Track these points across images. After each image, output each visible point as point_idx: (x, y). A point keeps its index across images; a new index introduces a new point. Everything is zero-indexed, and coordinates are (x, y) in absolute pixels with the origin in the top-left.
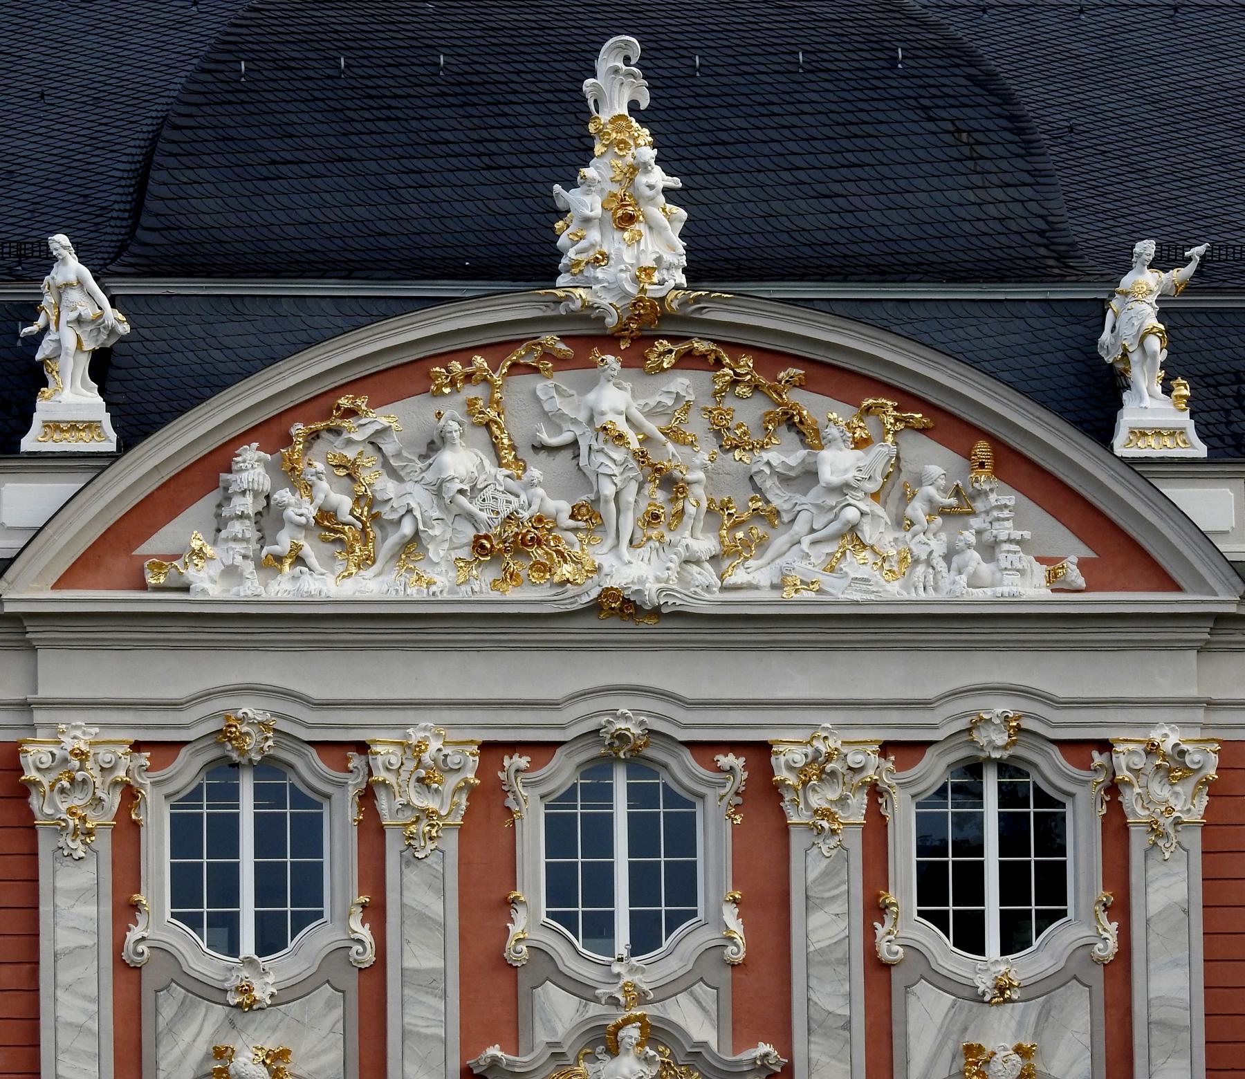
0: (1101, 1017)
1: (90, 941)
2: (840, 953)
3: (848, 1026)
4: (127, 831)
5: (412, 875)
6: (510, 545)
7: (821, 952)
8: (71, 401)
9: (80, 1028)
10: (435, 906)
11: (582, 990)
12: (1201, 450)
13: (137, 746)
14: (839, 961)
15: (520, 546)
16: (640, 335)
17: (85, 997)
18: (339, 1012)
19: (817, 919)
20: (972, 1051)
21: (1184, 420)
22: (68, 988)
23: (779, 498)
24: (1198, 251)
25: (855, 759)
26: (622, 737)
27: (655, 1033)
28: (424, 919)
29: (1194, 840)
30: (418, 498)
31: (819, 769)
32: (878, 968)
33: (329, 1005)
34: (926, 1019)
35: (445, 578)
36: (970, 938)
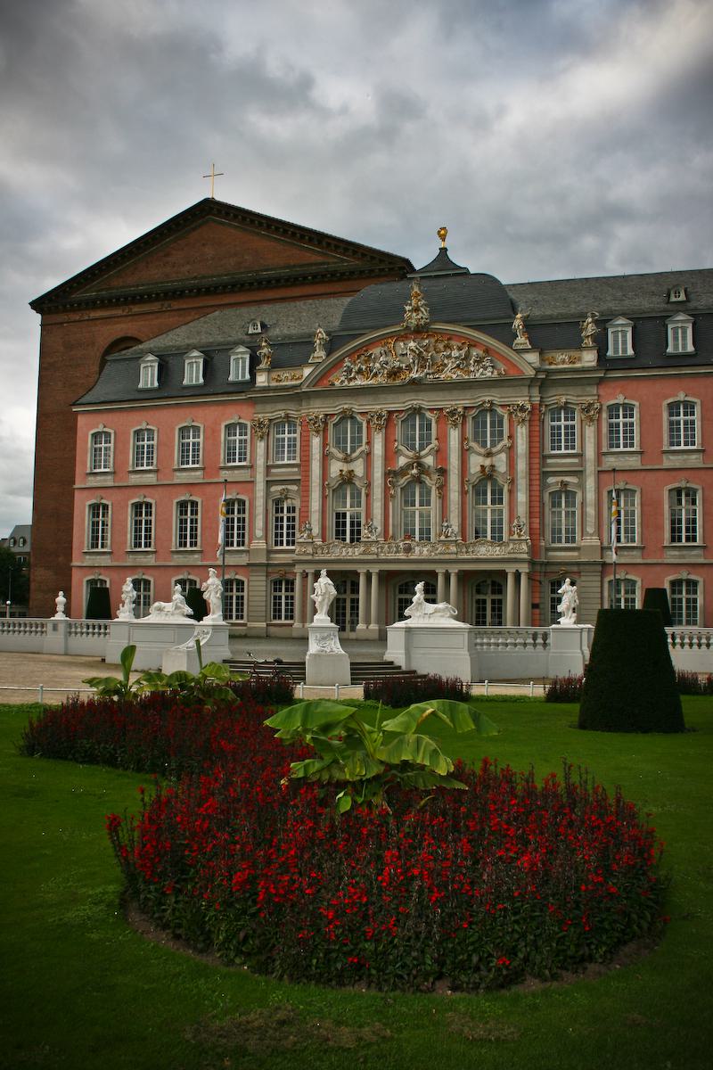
4: (325, 430)
6: (394, 373)
8: (320, 354)
11: (407, 457)
12: (530, 347)
13: (327, 415)
15: (395, 374)
16: (419, 331)
20: (482, 466)
21: (527, 341)
23: (446, 361)
25: (459, 410)
26: (415, 409)
27: (420, 465)
29: (527, 424)
30: (377, 365)
31: (452, 413)
32: (464, 453)
35: (381, 380)
36: (484, 444)
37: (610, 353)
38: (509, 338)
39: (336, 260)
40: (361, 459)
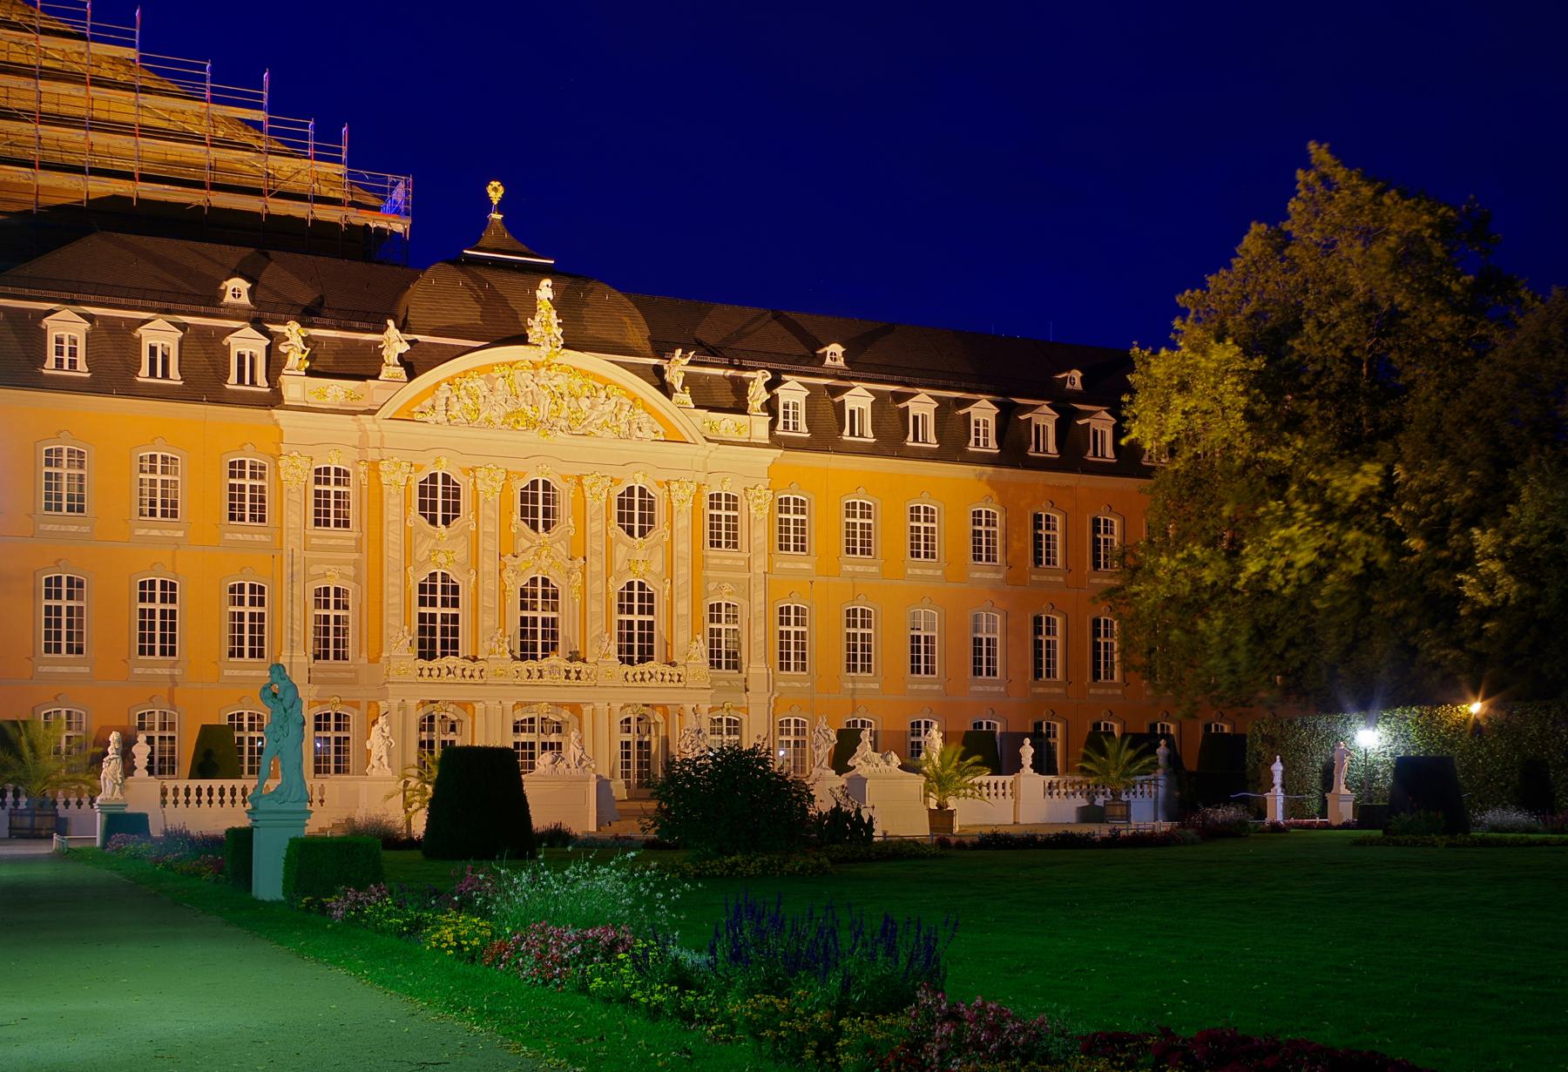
34: (621, 552)
37: (780, 426)
38: (666, 389)
39: (252, 170)
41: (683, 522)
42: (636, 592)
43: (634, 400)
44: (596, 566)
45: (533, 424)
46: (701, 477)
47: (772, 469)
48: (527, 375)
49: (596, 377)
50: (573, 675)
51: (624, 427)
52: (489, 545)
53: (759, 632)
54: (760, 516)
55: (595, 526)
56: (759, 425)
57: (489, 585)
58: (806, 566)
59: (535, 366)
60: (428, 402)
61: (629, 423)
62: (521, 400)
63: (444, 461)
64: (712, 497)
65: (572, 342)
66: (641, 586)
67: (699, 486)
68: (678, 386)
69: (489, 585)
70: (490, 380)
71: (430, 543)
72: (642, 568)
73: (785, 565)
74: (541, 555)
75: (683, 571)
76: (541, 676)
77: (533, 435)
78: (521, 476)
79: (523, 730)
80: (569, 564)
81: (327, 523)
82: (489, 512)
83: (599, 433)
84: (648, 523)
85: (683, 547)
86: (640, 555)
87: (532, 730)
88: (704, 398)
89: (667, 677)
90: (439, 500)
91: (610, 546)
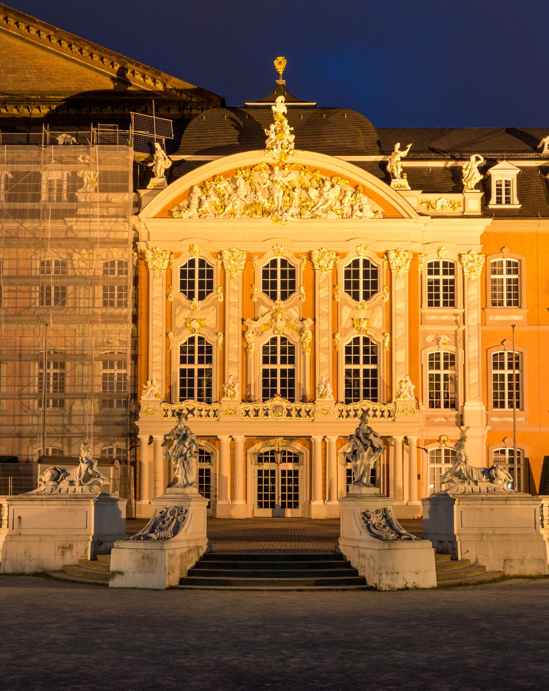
0: (385, 314)
1: (160, 295)
2: (326, 298)
3: (328, 315)
5: (232, 281)
7: (322, 298)
9: (158, 314)
10: (236, 288)
14: (326, 300)
17: (159, 308)
18: (215, 311)
19: (321, 291)
22: (155, 306)
24: (409, 146)
28: (234, 291)
33: (213, 310)
34: (346, 314)
40: (213, 307)
41: (400, 285)
42: (361, 346)
43: (356, 187)
44: (324, 324)
45: (266, 213)
46: (417, 248)
47: (485, 238)
48: (265, 175)
49: (324, 171)
50: (294, 413)
51: (347, 210)
52: (234, 313)
53: (474, 376)
54: (473, 277)
55: (323, 293)
56: (473, 201)
57: (234, 344)
58: (517, 318)
59: (271, 167)
60: (185, 203)
61: (352, 206)
62: (259, 193)
63: (196, 248)
64: (430, 265)
65: (301, 145)
66: (366, 340)
67: (416, 256)
68: (397, 173)
69: (234, 344)
70: (234, 181)
71: (186, 314)
72: (364, 325)
73: (498, 318)
74: (282, 318)
75: (401, 327)
76: (267, 414)
77: (267, 221)
78: (261, 256)
79: (266, 460)
80: (299, 325)
81: (437, 304)
82: (234, 286)
83: (324, 215)
84: (372, 287)
85: (401, 305)
86: (362, 314)
87: (273, 460)
88: (421, 182)
89: (378, 413)
90: (198, 280)
91: (336, 308)
